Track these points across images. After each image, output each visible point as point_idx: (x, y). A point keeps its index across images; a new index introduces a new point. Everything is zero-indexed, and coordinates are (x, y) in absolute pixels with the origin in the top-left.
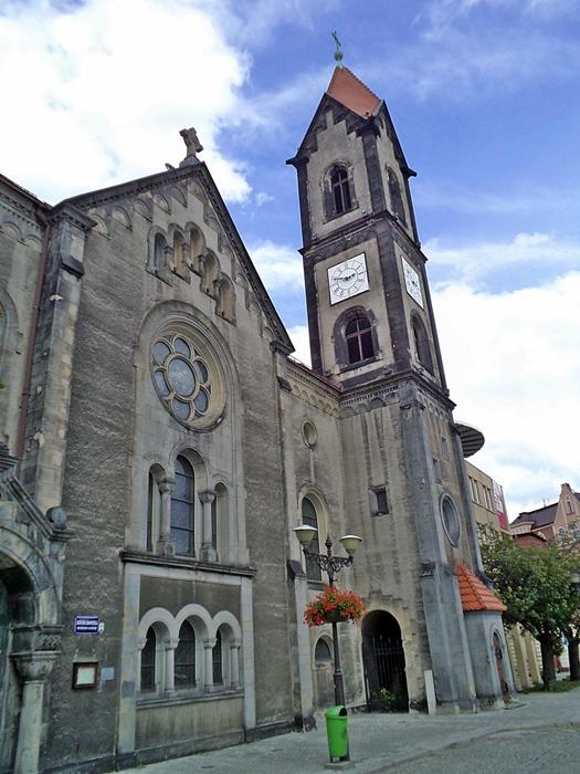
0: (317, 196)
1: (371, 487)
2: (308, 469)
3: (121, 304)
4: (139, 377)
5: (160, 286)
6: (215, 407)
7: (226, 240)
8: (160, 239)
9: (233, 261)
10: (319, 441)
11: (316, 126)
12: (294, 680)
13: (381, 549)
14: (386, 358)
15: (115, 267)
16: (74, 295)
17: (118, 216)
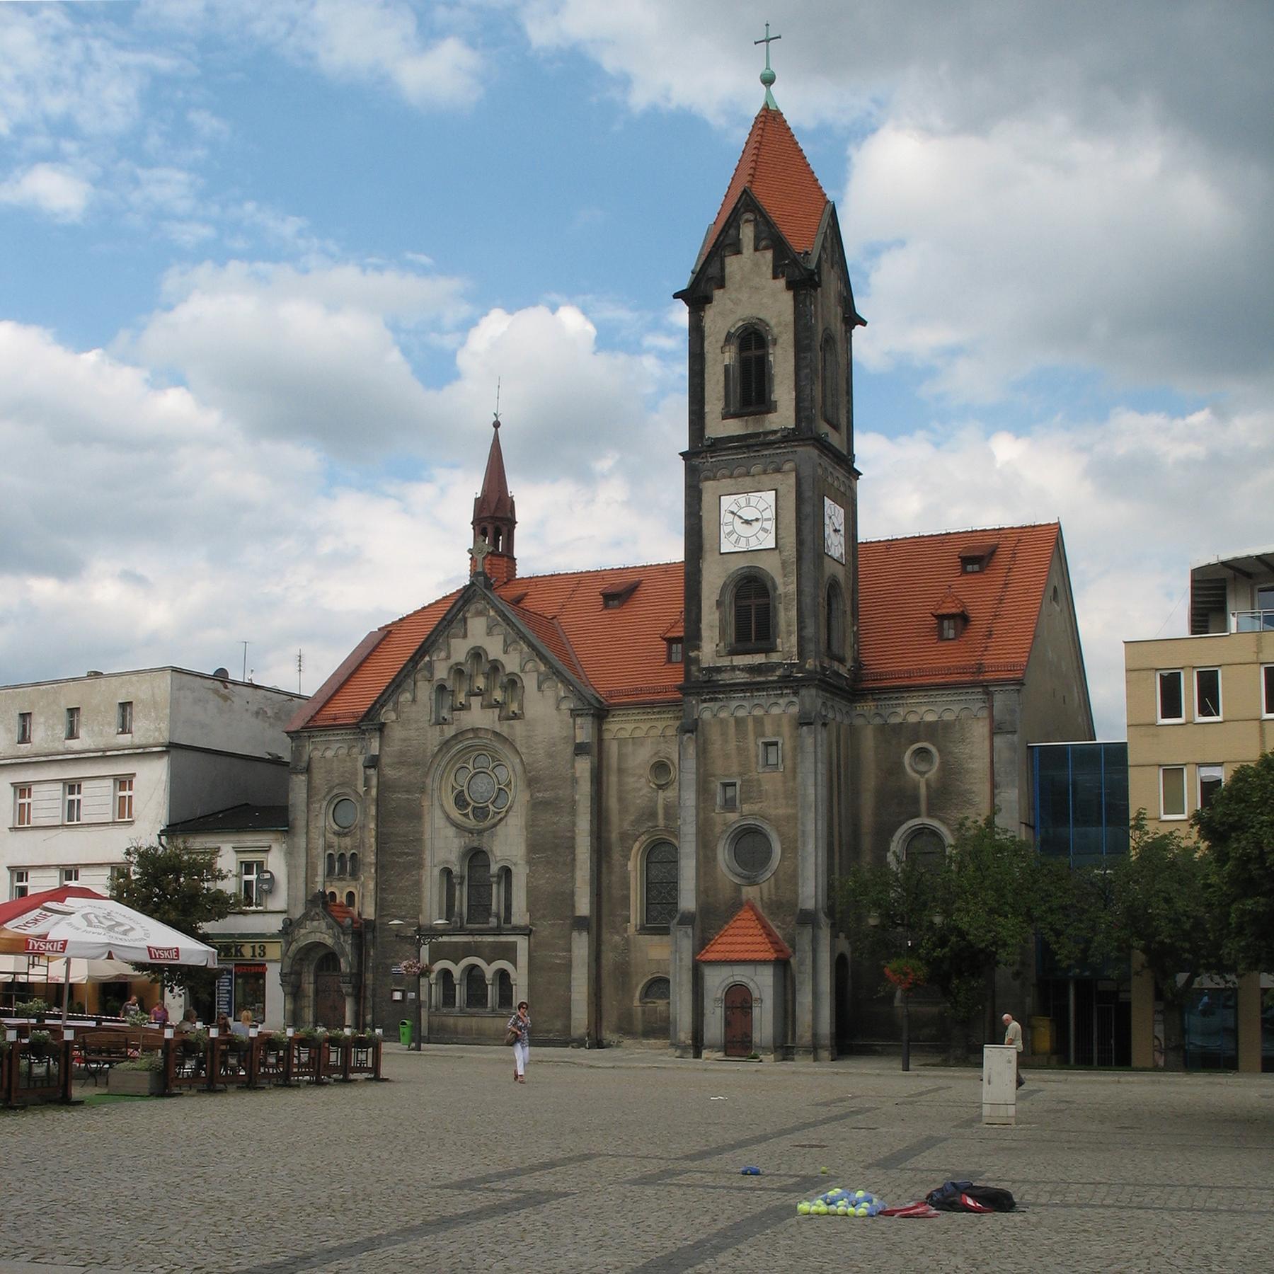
5: (442, 731)
8: (441, 688)
9: (521, 652)
15: (405, 740)
17: (406, 697)
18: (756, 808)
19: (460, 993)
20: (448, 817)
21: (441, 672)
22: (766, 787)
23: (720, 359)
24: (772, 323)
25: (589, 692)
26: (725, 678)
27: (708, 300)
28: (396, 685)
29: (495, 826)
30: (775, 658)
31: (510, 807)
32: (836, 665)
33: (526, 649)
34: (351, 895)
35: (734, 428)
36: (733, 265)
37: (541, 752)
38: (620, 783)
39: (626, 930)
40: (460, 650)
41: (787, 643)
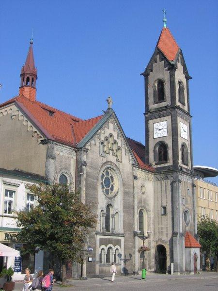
0: (151, 91)
1: (162, 206)
2: (142, 201)
6: (115, 189)
7: (120, 134)
10: (146, 191)
11: (153, 60)
12: (134, 263)
13: (163, 226)
14: (170, 163)
16: (85, 172)
17: (93, 142)
21: (103, 138)
33: (123, 140)
37: (126, 175)
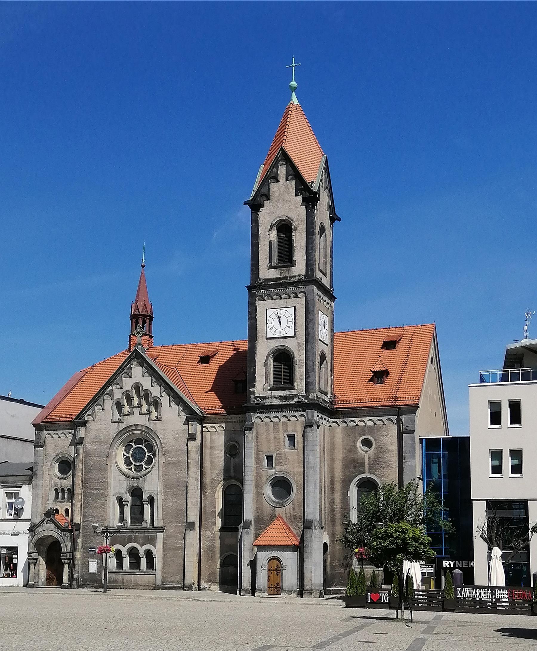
3: (101, 442)
4: (109, 467)
5: (118, 426)
16: (81, 451)
18: (283, 468)
19: (126, 561)
20: (120, 471)
21: (118, 395)
22: (288, 457)
23: (269, 237)
24: (295, 219)
25: (195, 408)
26: (269, 402)
27: (261, 206)
28: (94, 401)
29: (146, 475)
30: (293, 392)
31: (154, 465)
32: (323, 396)
34: (67, 511)
35: (274, 274)
36: (274, 187)
38: (211, 454)
39: (213, 529)
40: (128, 384)
41: (300, 385)
